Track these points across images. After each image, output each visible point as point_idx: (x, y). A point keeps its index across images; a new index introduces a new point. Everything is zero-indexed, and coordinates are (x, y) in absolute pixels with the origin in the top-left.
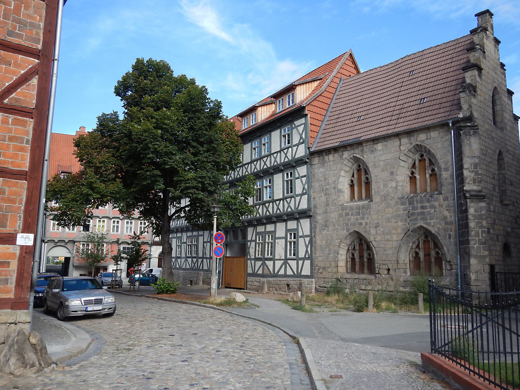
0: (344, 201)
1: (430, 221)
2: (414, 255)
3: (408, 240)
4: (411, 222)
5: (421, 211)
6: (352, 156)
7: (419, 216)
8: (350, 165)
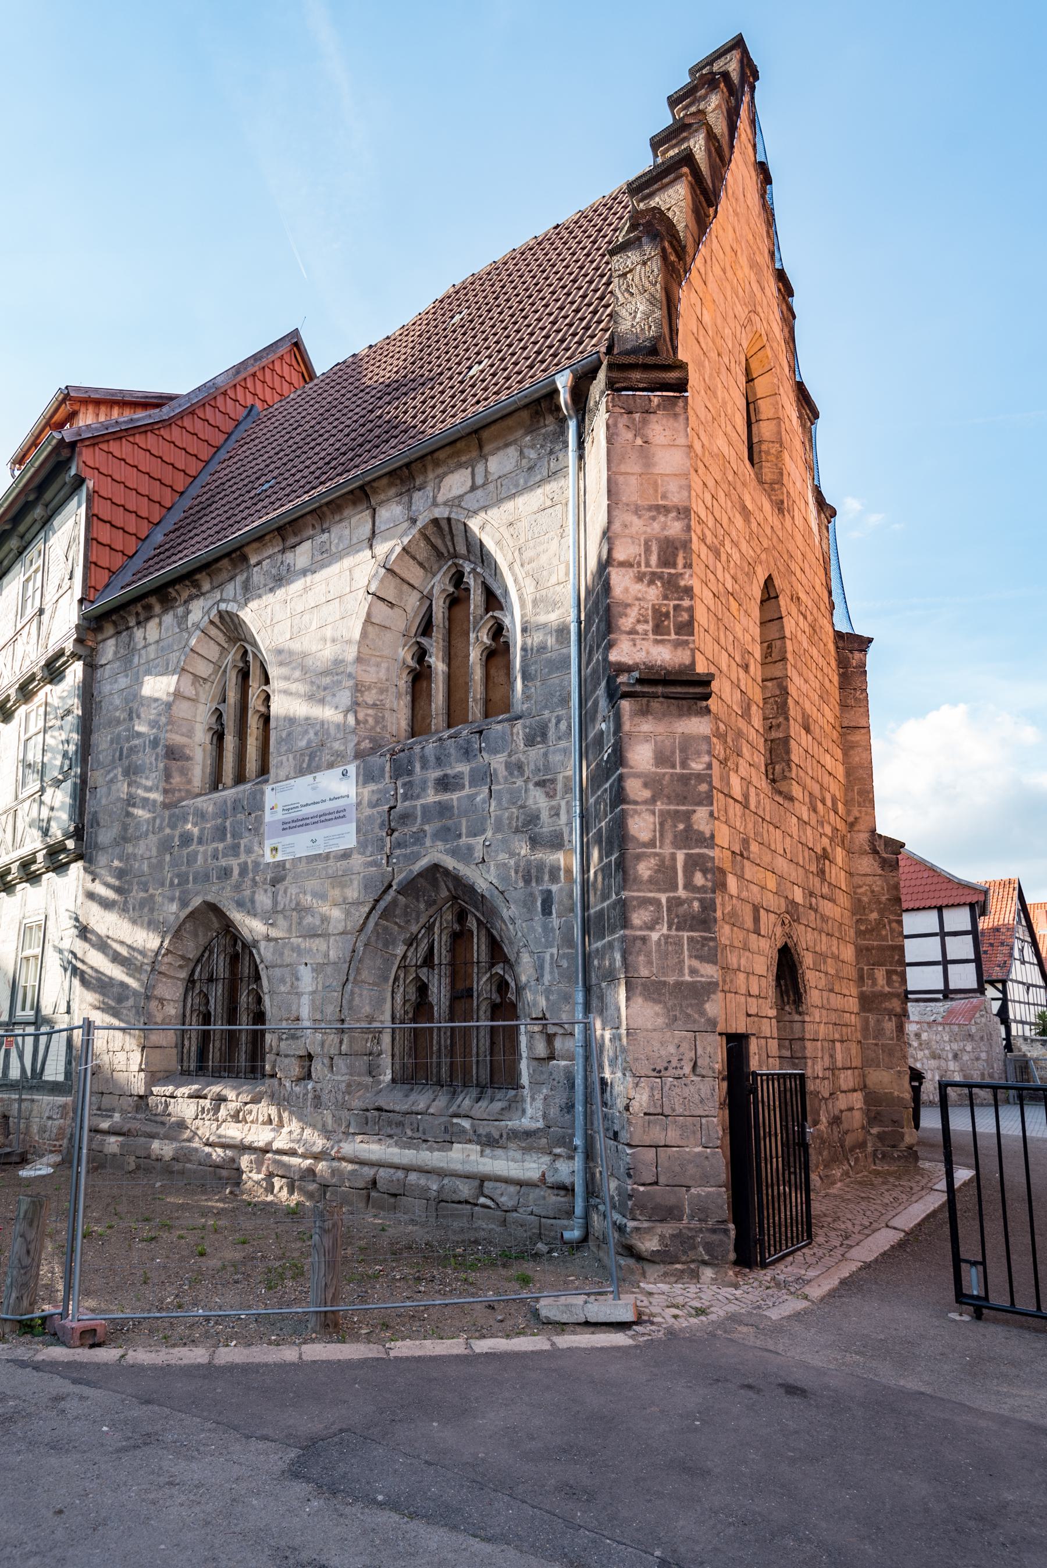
0: (188, 791)
1: (471, 841)
2: (413, 996)
3: (386, 928)
4: (397, 852)
5: (437, 798)
6: (214, 611)
7: (428, 822)
8: (212, 651)
